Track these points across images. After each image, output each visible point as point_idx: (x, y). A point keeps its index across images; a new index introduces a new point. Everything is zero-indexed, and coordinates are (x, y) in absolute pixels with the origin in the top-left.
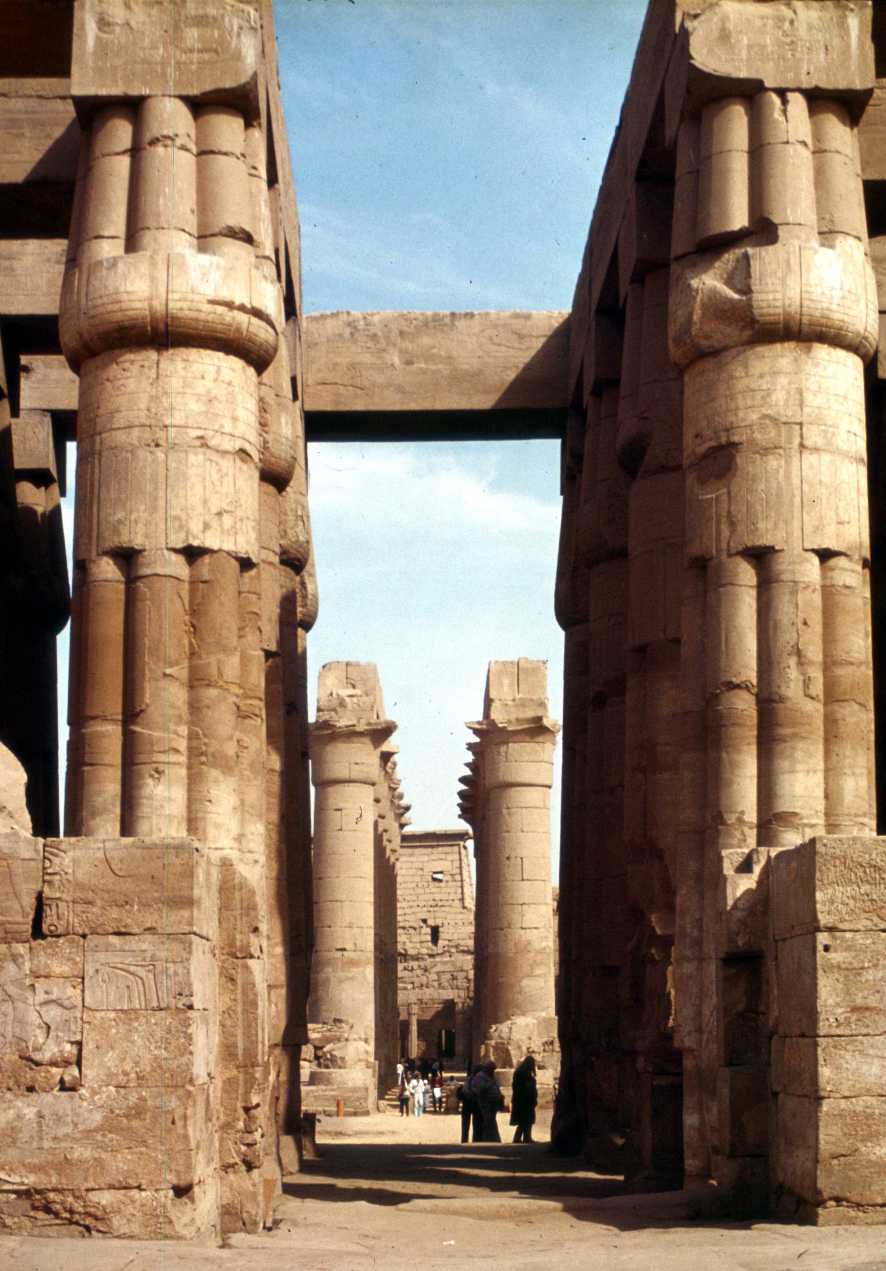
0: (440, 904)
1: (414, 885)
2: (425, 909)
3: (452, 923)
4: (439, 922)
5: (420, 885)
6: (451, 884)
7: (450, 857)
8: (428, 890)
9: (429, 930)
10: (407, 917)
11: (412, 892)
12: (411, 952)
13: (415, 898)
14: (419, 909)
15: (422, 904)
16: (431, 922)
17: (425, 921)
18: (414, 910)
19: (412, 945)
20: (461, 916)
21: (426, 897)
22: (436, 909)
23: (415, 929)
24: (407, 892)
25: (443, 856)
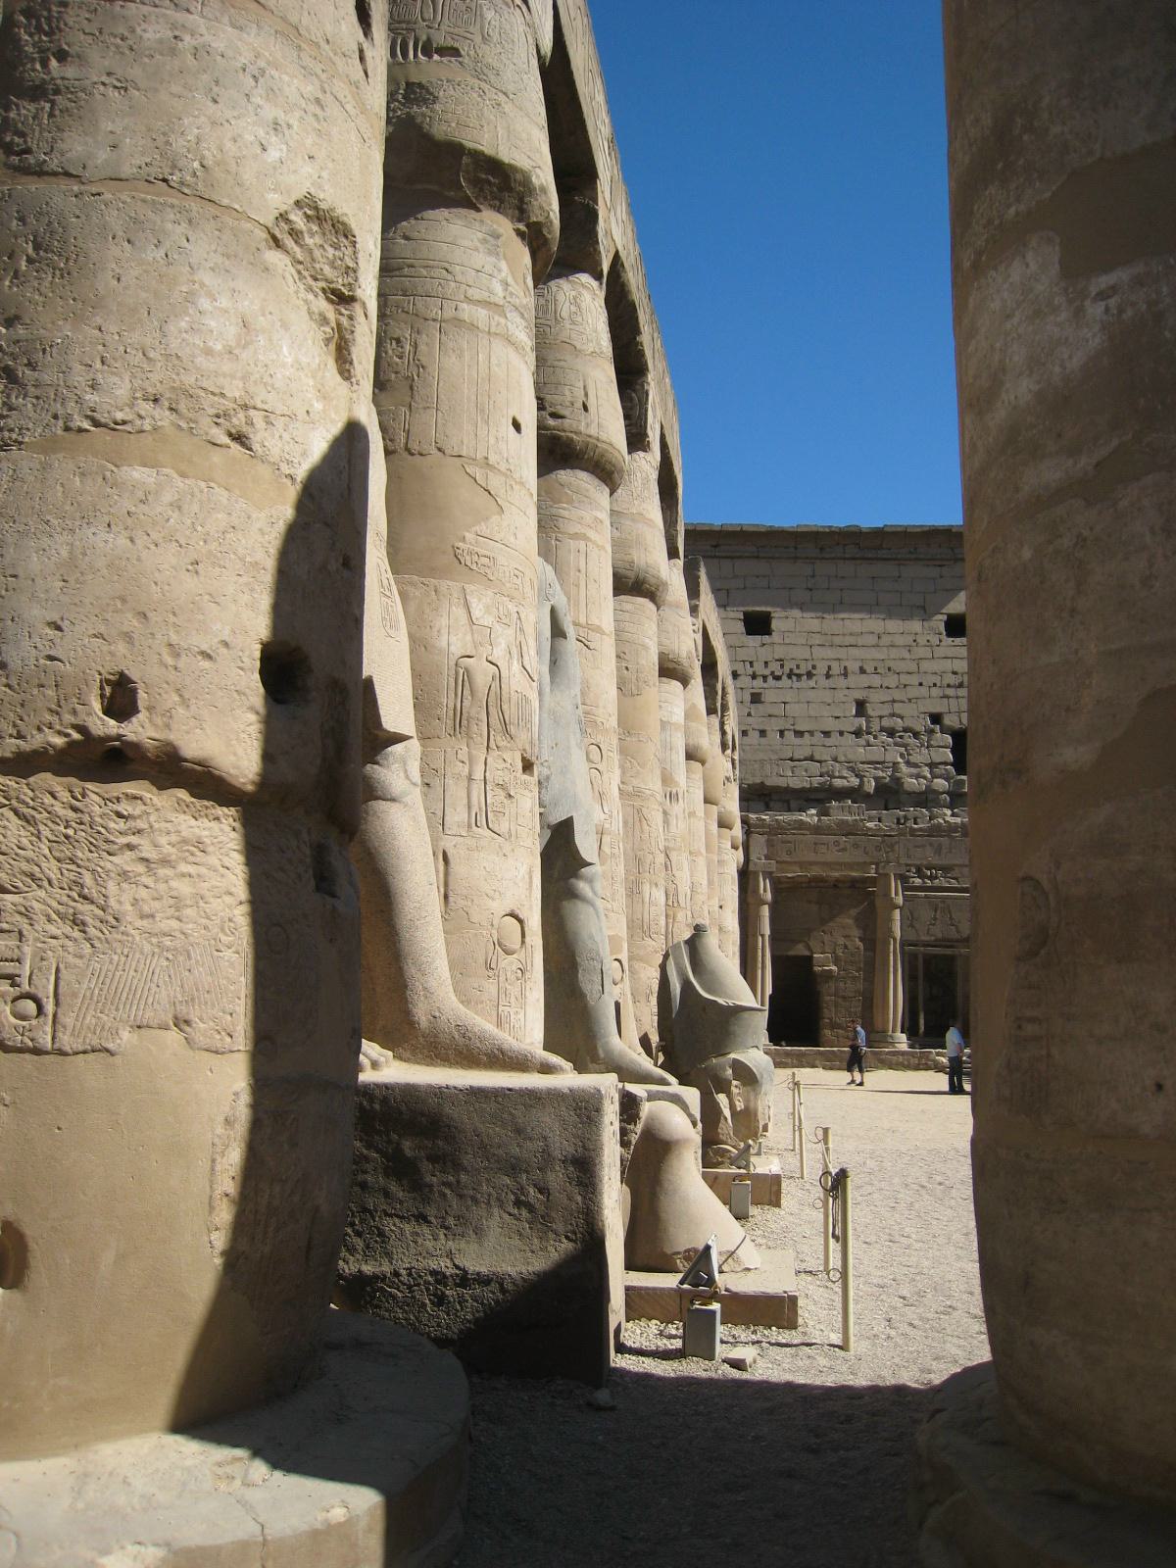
1: (909, 640)
2: (935, 692)
5: (922, 640)
8: (940, 652)
9: (949, 739)
10: (898, 708)
11: (907, 656)
12: (911, 784)
13: (913, 667)
14: (924, 691)
15: (930, 680)
17: (936, 718)
18: (913, 692)
19: (914, 771)
21: (935, 666)
23: (916, 735)
24: (894, 653)
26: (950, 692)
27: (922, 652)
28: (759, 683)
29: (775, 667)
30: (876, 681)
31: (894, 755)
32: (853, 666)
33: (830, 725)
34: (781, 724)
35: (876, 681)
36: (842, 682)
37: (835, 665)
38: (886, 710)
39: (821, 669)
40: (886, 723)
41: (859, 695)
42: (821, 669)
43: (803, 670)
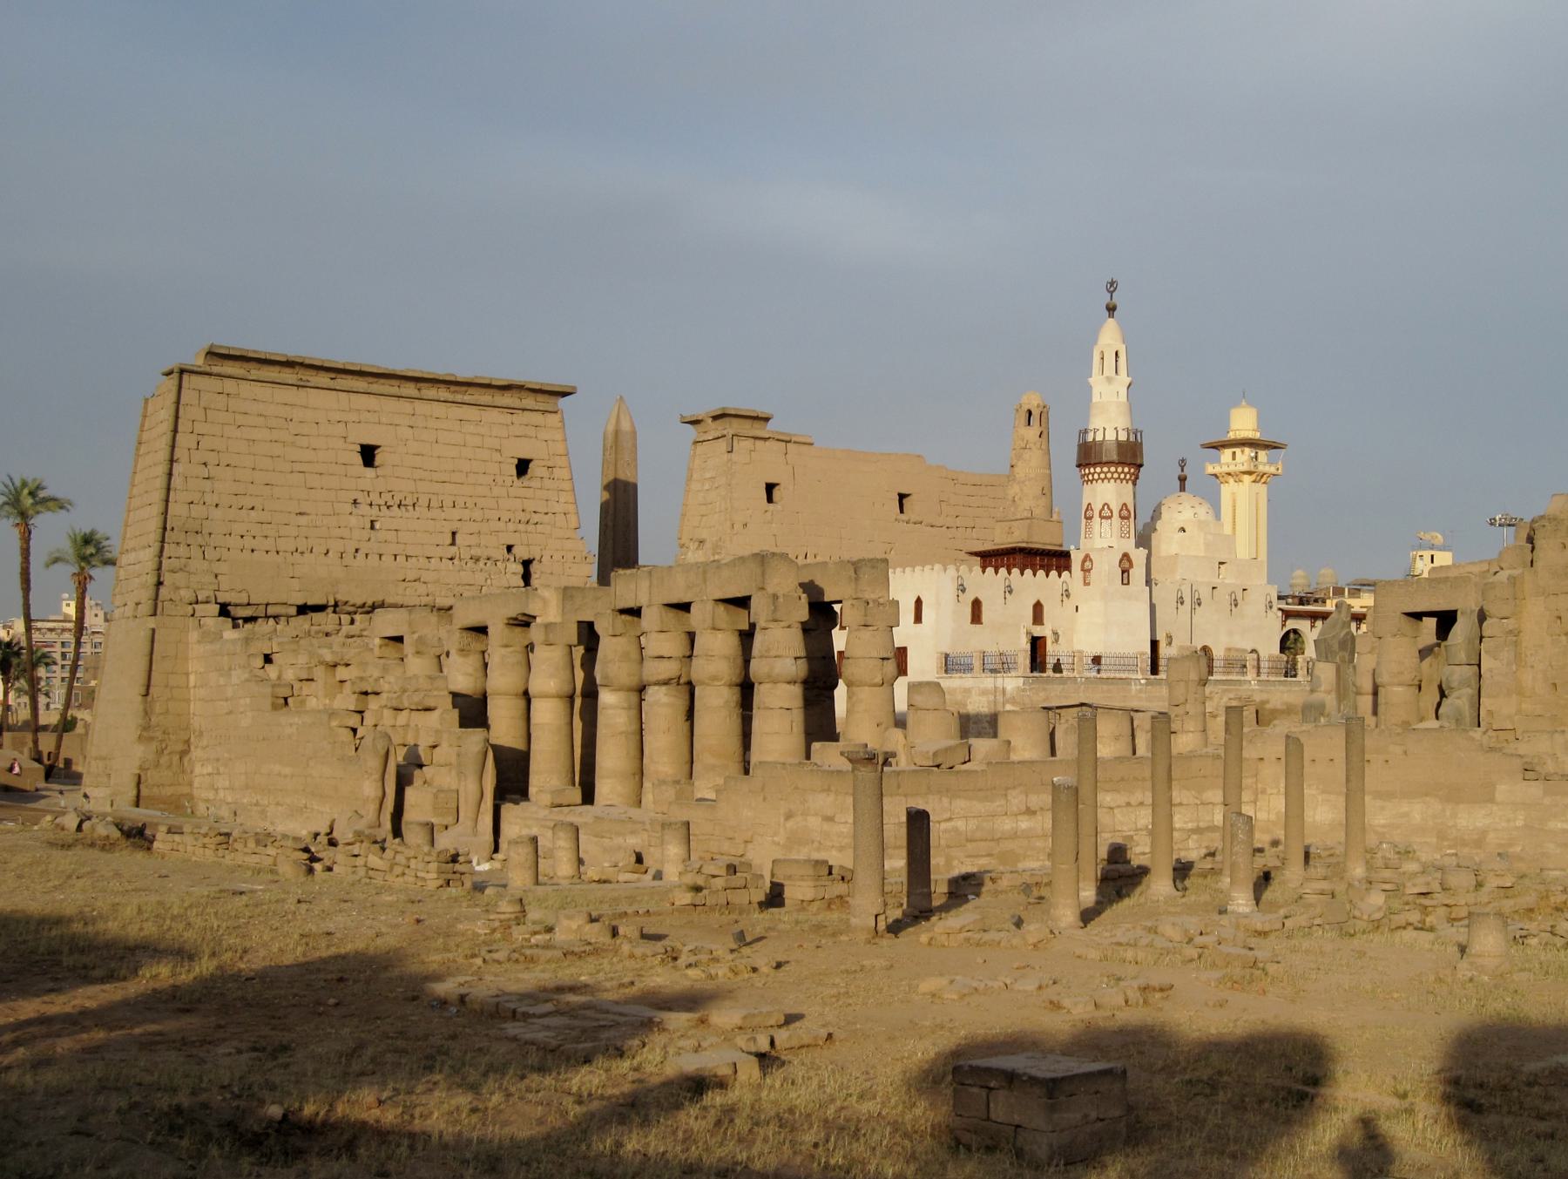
0: (536, 518)
1: (489, 479)
2: (511, 526)
3: (557, 556)
4: (534, 553)
5: (499, 480)
6: (547, 483)
7: (543, 435)
14: (501, 525)
16: (521, 552)
20: (569, 544)
22: (531, 528)
25: (531, 432)
26: (521, 527)
27: (496, 491)
28: (375, 510)
29: (387, 497)
30: (466, 514)
31: (480, 578)
32: (448, 503)
33: (431, 551)
34: (394, 549)
35: (466, 514)
36: (435, 513)
37: (434, 498)
38: (473, 540)
39: (423, 501)
40: (475, 552)
41: (454, 526)
42: (423, 501)
43: (409, 501)
